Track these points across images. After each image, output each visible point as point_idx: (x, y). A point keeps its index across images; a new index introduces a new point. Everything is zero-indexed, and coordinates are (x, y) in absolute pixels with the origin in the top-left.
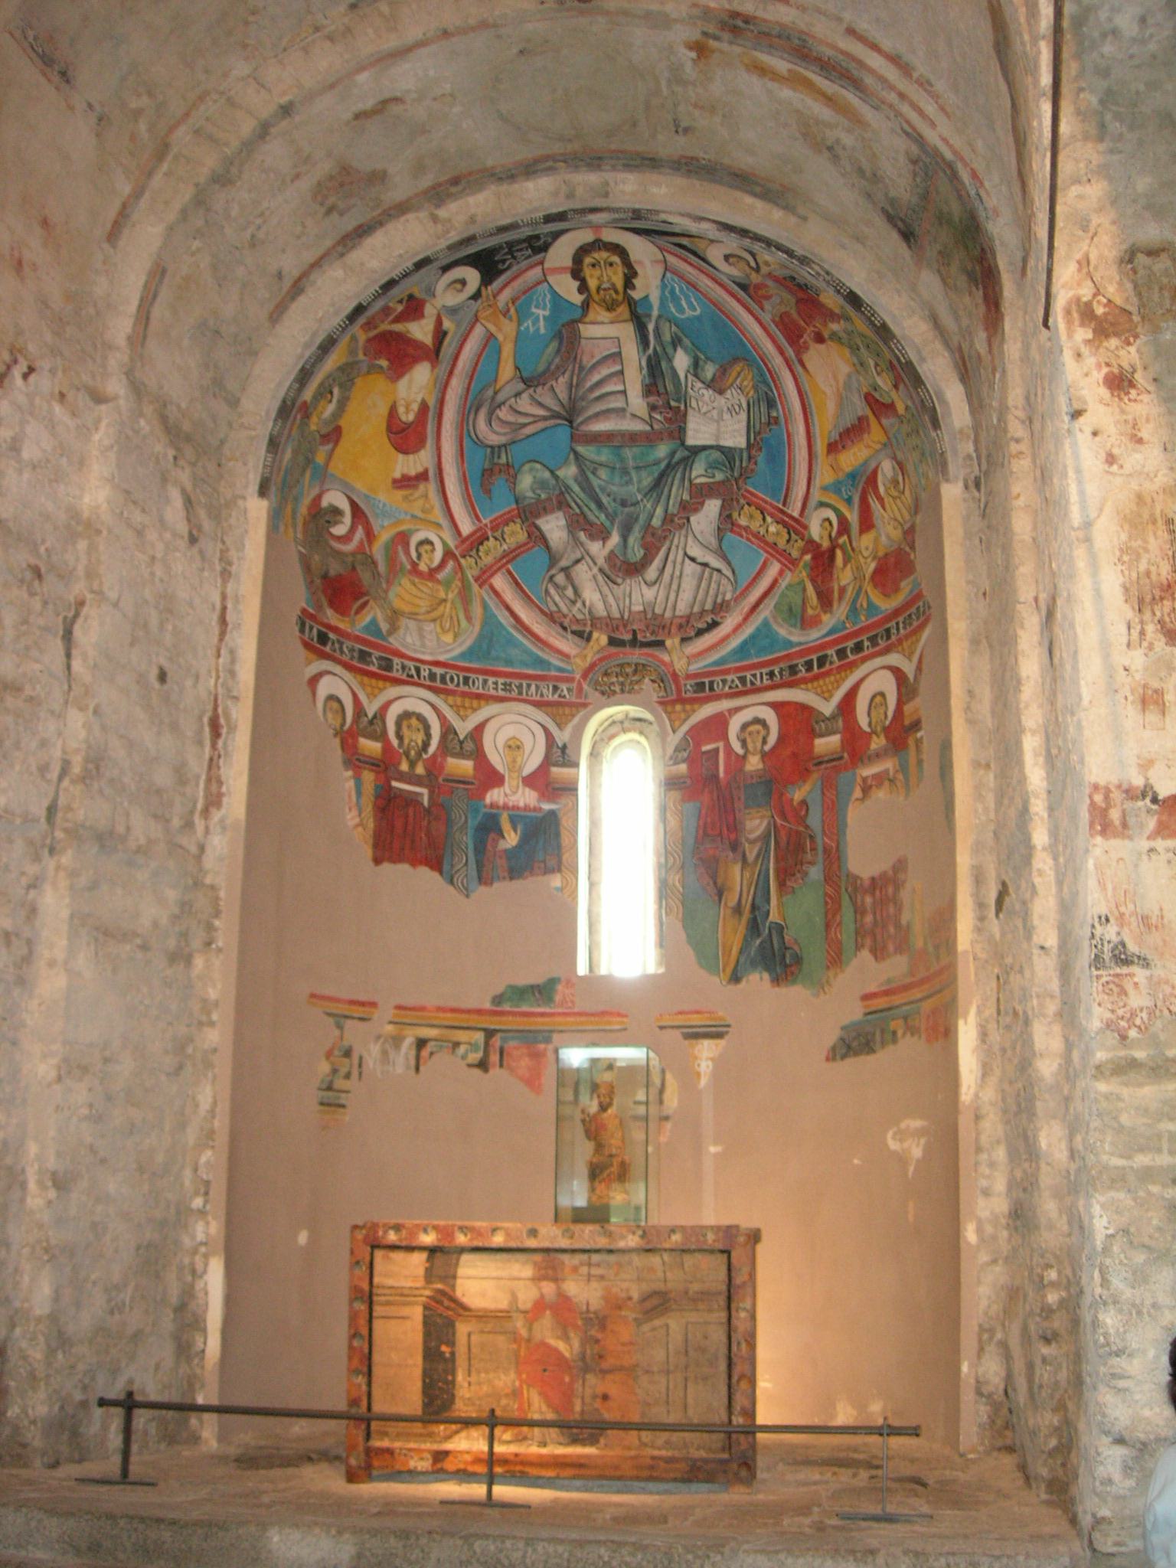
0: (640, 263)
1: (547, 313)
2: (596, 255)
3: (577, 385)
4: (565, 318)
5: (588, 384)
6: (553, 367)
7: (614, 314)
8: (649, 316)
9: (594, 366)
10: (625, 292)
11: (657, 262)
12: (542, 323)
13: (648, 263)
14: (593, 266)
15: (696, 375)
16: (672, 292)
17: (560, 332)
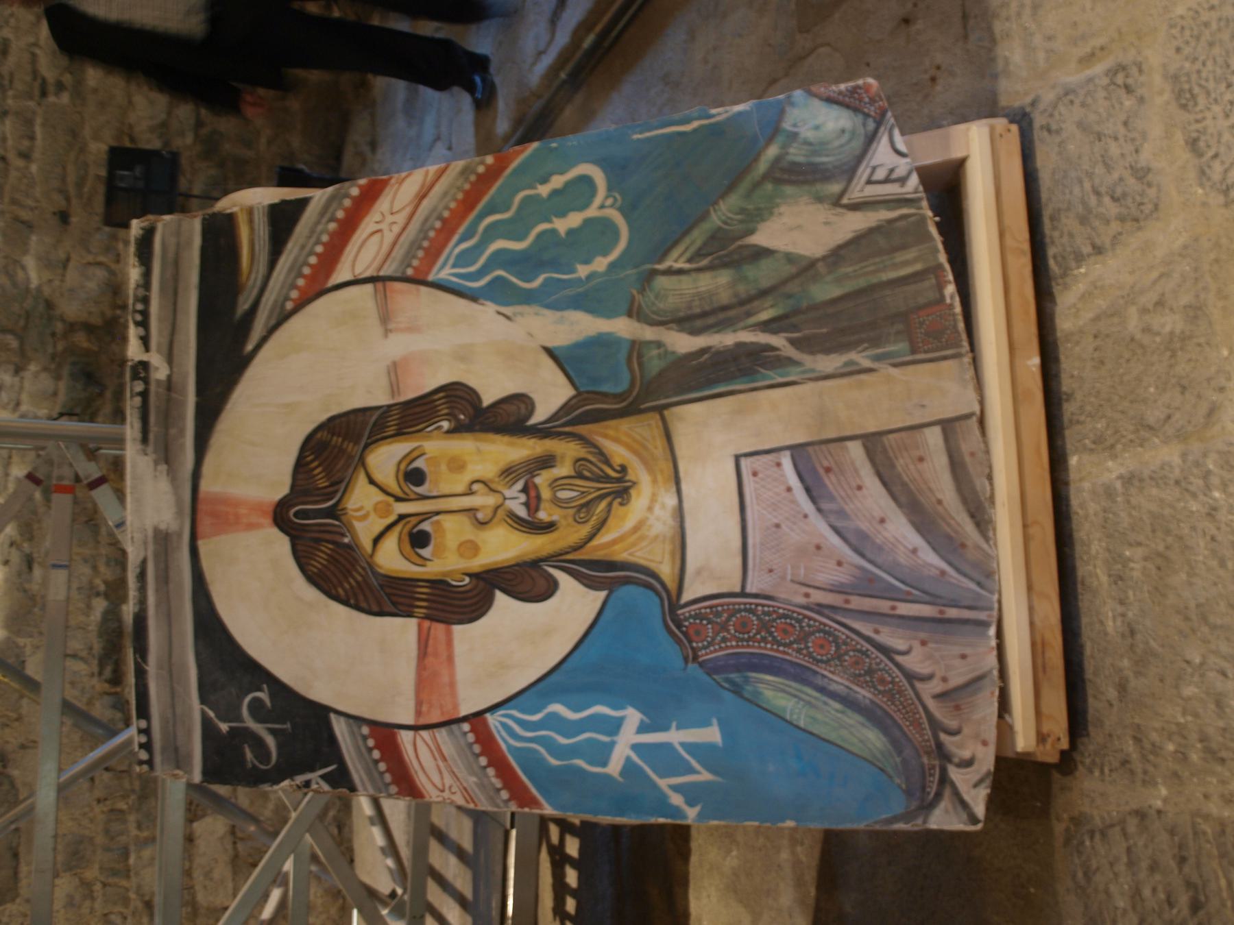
0: (395, 371)
1: (633, 716)
2: (365, 531)
3: (932, 598)
4: (670, 653)
5: (930, 557)
6: (864, 694)
7: (639, 473)
8: (637, 348)
9: (859, 542)
10: (541, 432)
11: (385, 318)
12: (674, 736)
13: (397, 346)
14: (419, 540)
15: (849, 171)
16: (525, 263)
17: (712, 669)
